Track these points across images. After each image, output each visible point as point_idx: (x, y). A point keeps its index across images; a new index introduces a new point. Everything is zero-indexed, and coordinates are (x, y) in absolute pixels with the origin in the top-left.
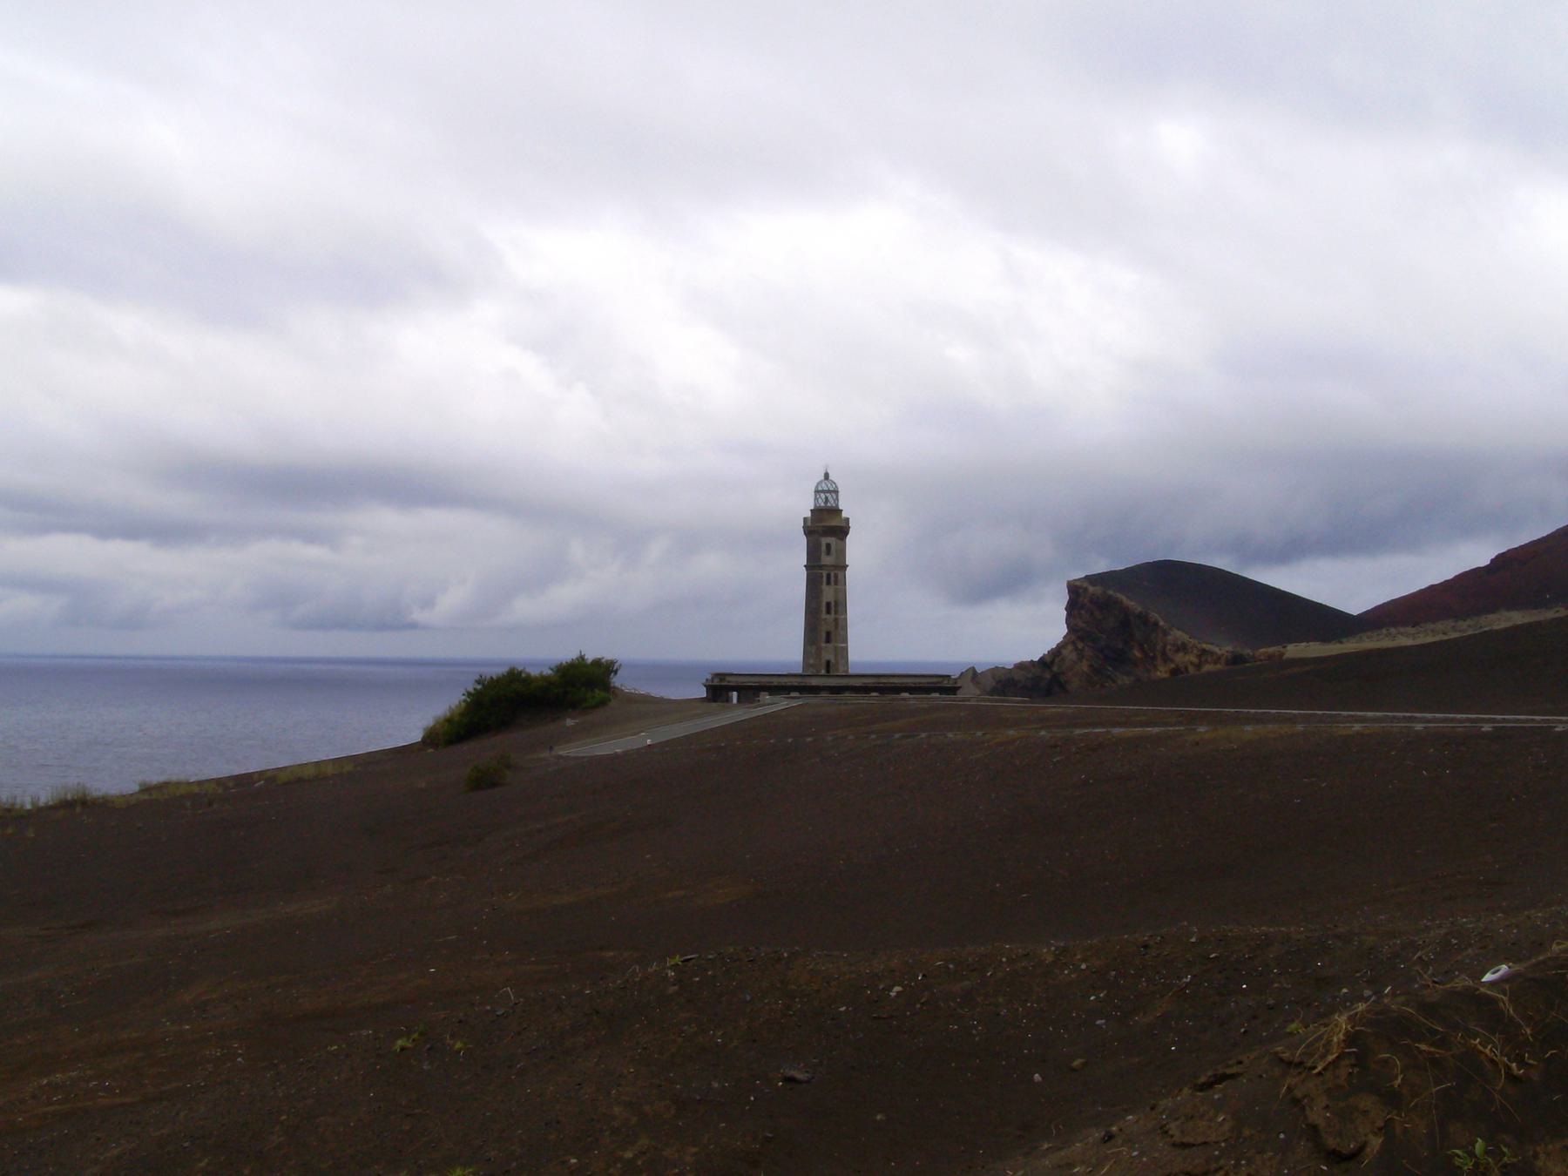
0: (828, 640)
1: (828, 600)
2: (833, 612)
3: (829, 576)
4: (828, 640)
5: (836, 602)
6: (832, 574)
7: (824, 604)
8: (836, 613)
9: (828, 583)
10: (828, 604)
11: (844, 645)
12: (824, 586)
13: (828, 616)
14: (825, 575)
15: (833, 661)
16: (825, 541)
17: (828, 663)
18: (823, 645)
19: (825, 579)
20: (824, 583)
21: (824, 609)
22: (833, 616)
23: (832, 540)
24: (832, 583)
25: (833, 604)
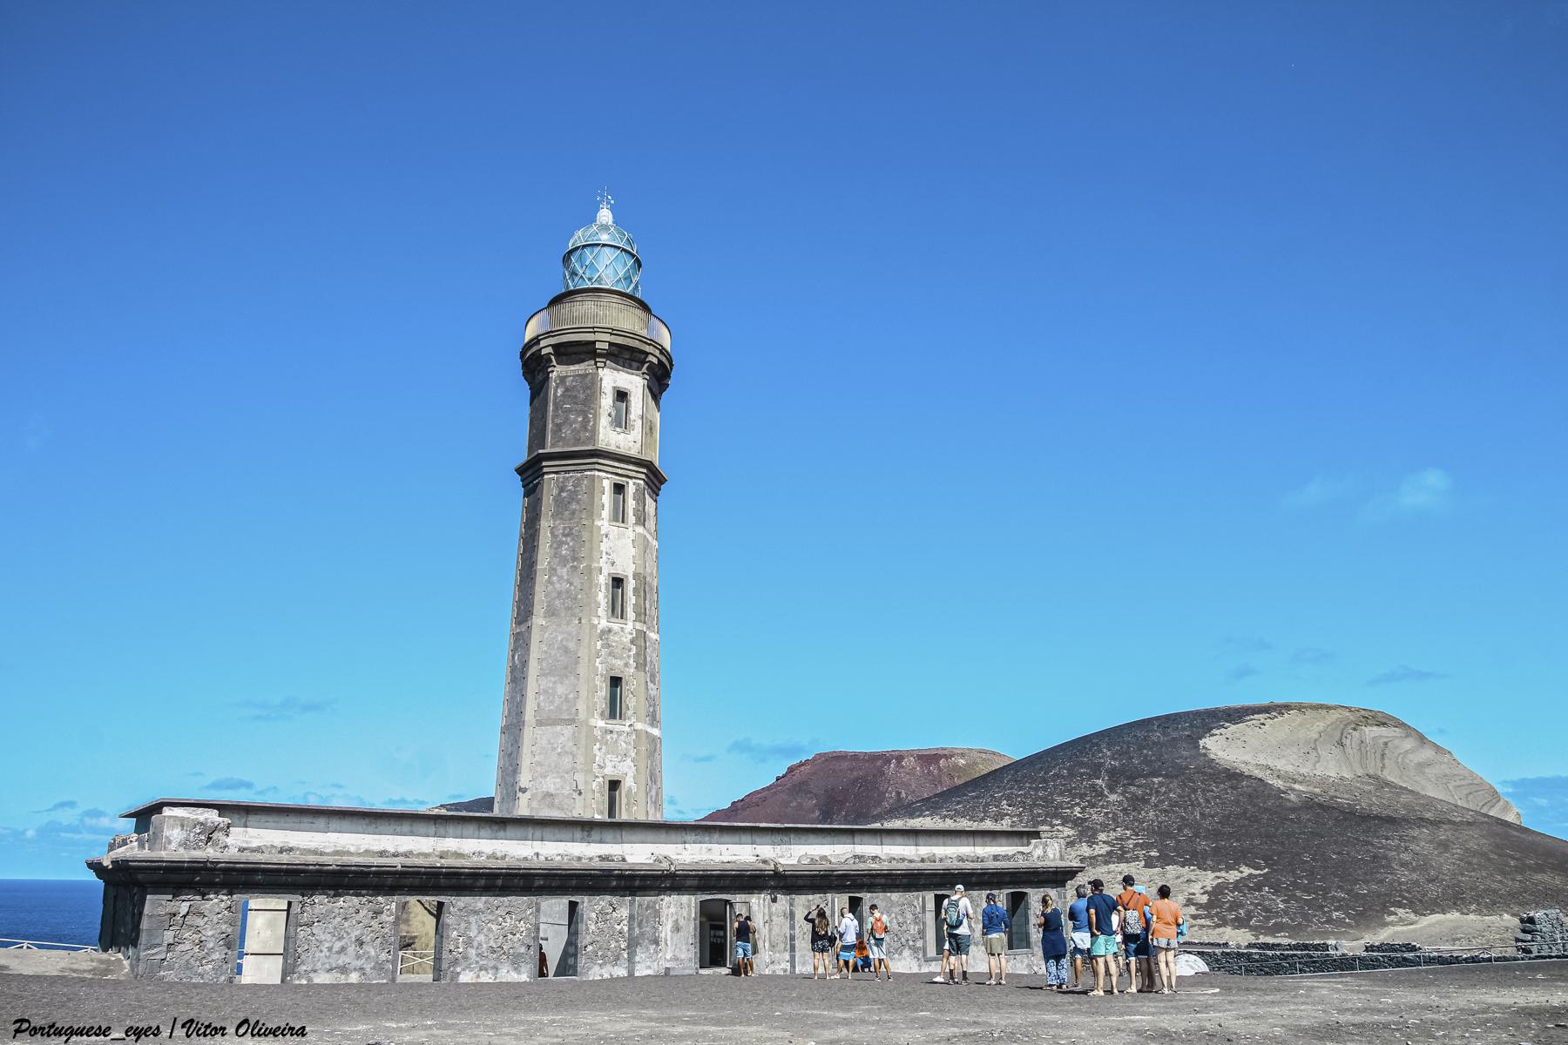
0: (614, 709)
1: (619, 571)
2: (631, 614)
3: (619, 489)
4: (614, 709)
5: (636, 576)
6: (631, 489)
7: (603, 580)
8: (641, 615)
9: (619, 516)
10: (618, 582)
11: (655, 732)
12: (604, 522)
13: (616, 627)
14: (607, 485)
15: (628, 783)
16: (611, 378)
17: (614, 785)
18: (601, 723)
19: (607, 498)
20: (606, 513)
21: (602, 597)
22: (630, 626)
23: (634, 383)
24: (631, 518)
25: (630, 585)
